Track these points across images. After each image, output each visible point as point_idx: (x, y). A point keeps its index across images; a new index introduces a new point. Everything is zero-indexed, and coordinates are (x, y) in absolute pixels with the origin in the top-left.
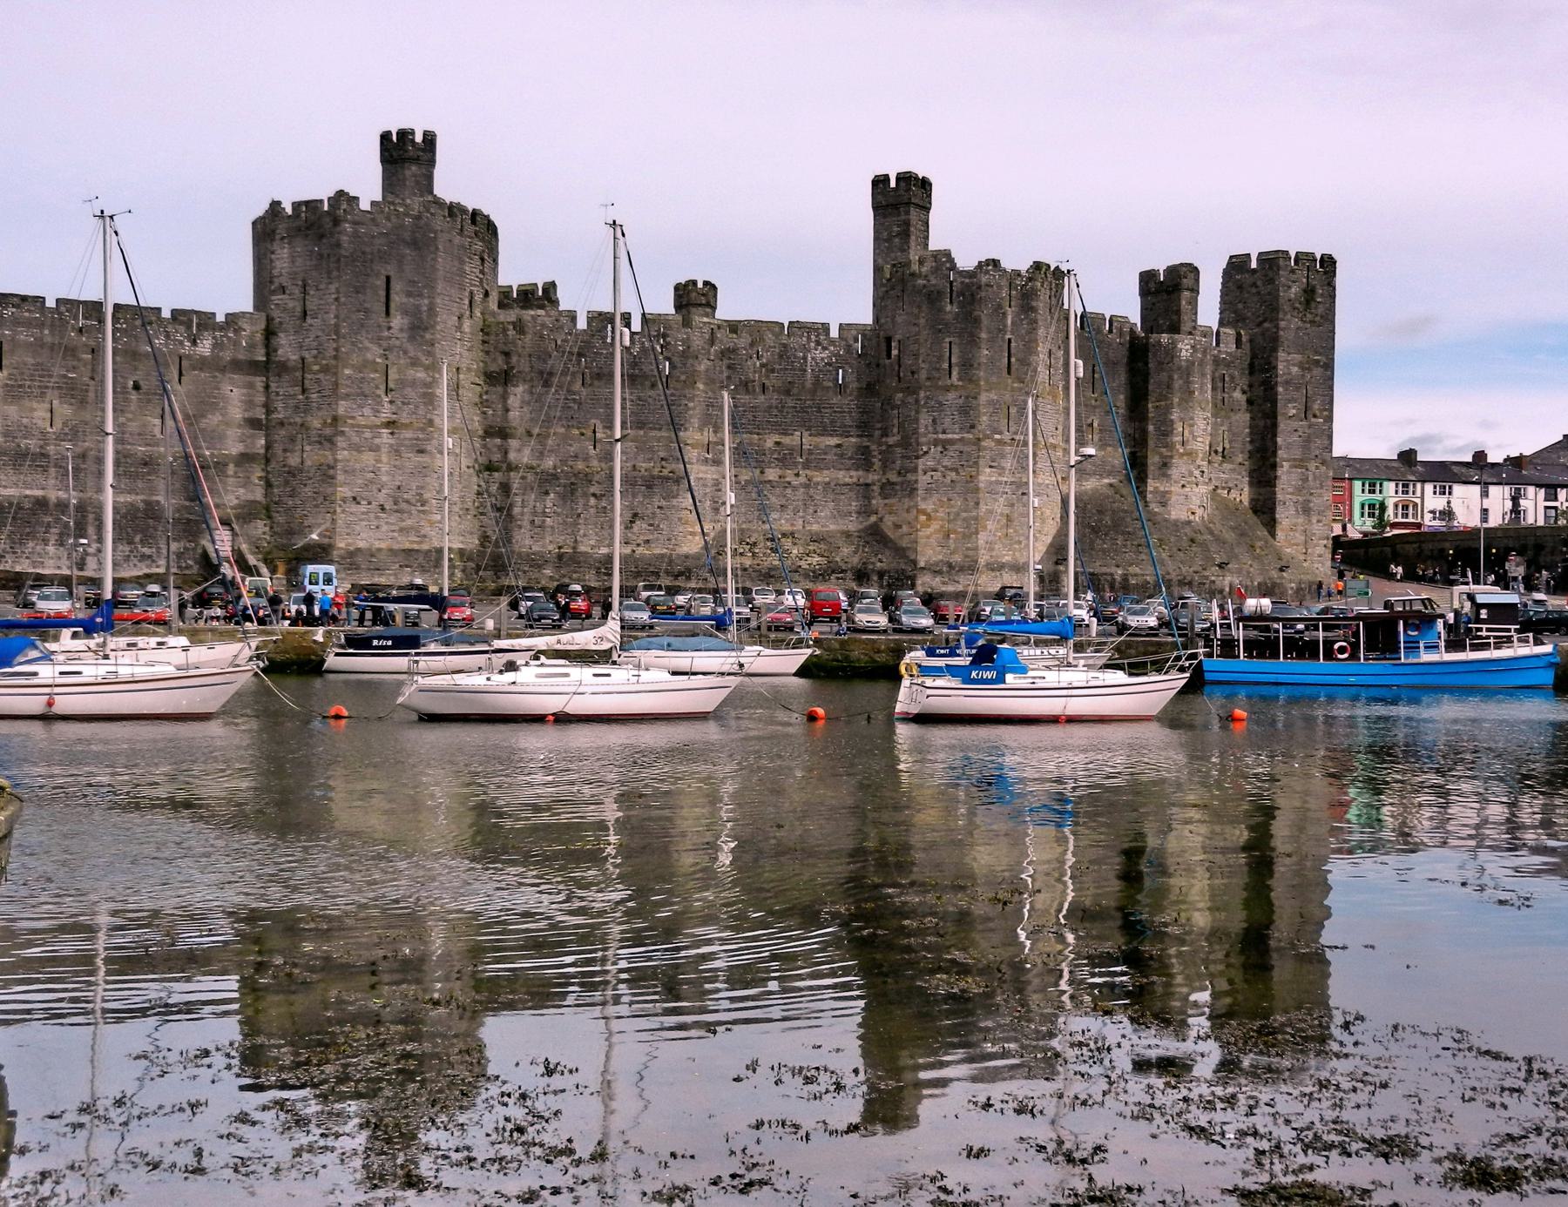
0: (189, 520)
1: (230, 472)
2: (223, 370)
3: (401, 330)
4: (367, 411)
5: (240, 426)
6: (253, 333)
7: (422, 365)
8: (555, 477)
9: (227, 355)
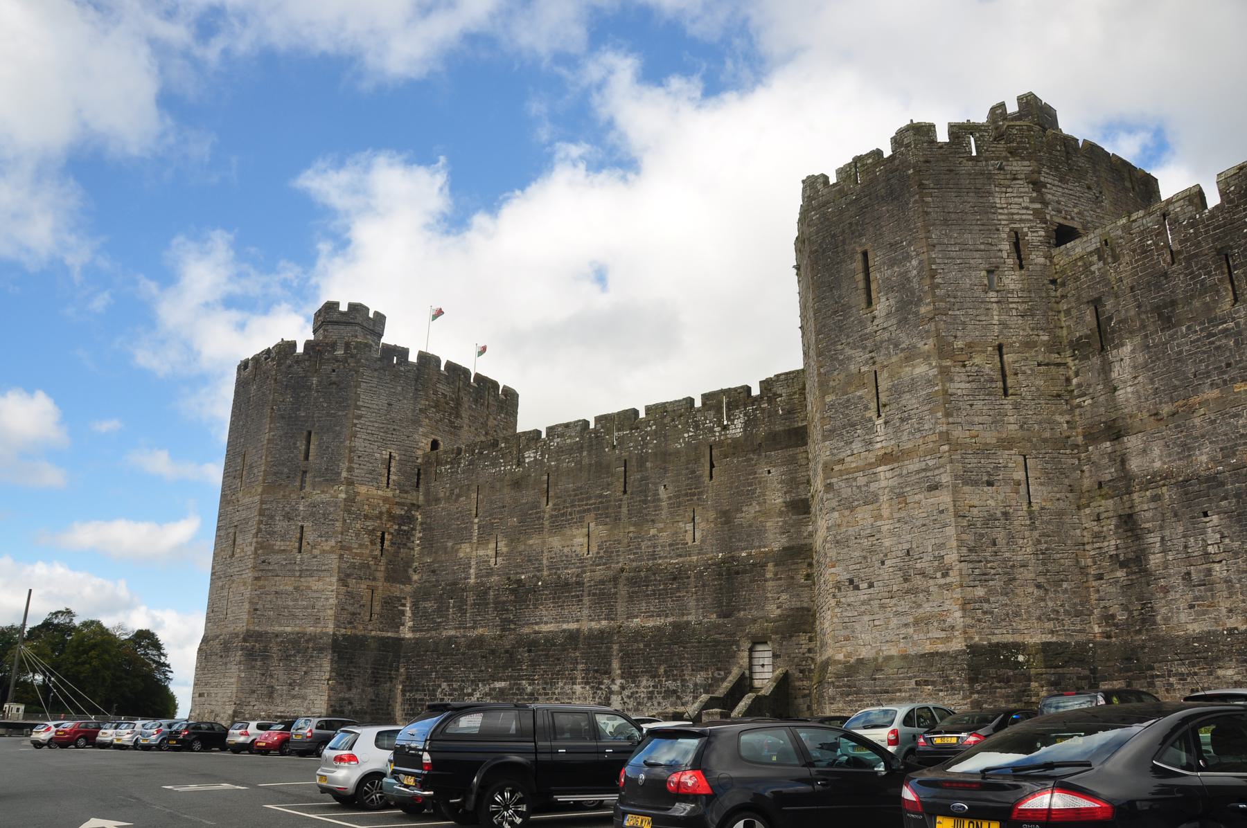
0: (717, 642)
1: (769, 575)
2: (758, 449)
3: (888, 315)
4: (857, 446)
5: (781, 513)
6: (790, 396)
7: (920, 355)
8: (1213, 481)
9: (762, 430)
